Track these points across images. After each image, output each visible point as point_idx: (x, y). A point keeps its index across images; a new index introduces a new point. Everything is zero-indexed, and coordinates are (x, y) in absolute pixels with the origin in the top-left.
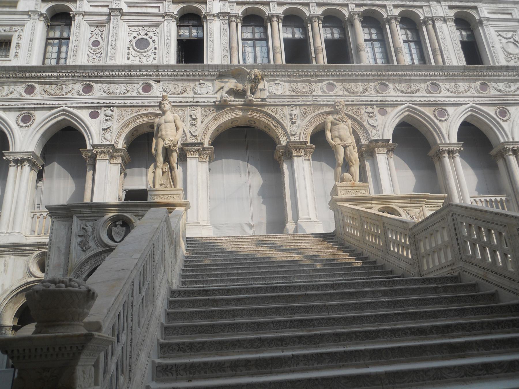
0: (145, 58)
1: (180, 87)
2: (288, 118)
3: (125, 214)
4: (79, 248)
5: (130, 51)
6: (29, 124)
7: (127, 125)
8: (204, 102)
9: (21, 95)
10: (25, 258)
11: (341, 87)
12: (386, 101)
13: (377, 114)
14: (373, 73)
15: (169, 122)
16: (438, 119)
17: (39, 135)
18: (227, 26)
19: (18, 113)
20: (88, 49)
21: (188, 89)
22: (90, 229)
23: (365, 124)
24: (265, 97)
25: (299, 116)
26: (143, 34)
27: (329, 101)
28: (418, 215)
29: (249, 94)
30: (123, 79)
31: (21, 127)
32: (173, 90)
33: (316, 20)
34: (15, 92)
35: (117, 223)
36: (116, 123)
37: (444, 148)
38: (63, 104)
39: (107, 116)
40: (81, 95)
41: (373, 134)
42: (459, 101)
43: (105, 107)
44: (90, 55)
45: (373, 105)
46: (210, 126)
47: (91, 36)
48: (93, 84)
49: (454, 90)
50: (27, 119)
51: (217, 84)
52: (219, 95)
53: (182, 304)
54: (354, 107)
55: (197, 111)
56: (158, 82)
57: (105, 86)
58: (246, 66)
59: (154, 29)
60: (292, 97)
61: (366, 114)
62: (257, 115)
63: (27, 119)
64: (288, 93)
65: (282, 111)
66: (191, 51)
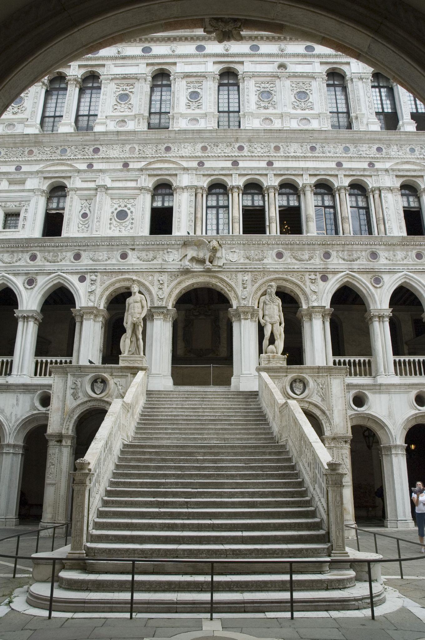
0: (124, 228)
1: (151, 255)
2: (241, 283)
3: (103, 374)
4: (72, 397)
5: (111, 222)
6: (32, 286)
7: (107, 289)
8: (170, 268)
9: (27, 262)
10: (32, 395)
11: (290, 254)
12: (328, 268)
13: (319, 281)
14: (319, 243)
15: (137, 302)
16: (374, 286)
17: (40, 296)
18: (193, 198)
19: (24, 277)
20: (78, 220)
21: (158, 256)
22: (79, 384)
23: (307, 290)
24: (222, 265)
25: (250, 281)
26: (123, 205)
27: (277, 268)
28: (323, 382)
29: (207, 263)
30: (105, 247)
31: (28, 289)
32: (145, 257)
33: (273, 191)
34: (23, 259)
35: (98, 380)
36: (99, 286)
37: (375, 314)
38: (58, 270)
39: (92, 281)
40: (72, 262)
41: (313, 299)
42: (394, 269)
43: (90, 272)
44: (80, 226)
45: (316, 271)
46: (174, 290)
47: (81, 208)
48: (82, 252)
49: (391, 258)
50: (31, 282)
51: (182, 252)
52: (182, 263)
53: (127, 452)
54: (299, 274)
55: (164, 276)
56: (133, 249)
57: (91, 254)
58: (206, 237)
59: (132, 201)
60: (245, 264)
61: (310, 280)
62: (214, 281)
63: (31, 282)
64: (242, 261)
65: (236, 277)
66: (161, 221)
